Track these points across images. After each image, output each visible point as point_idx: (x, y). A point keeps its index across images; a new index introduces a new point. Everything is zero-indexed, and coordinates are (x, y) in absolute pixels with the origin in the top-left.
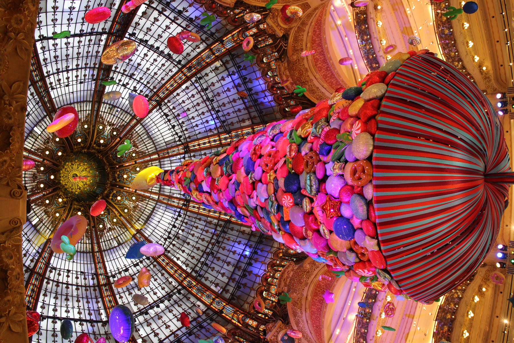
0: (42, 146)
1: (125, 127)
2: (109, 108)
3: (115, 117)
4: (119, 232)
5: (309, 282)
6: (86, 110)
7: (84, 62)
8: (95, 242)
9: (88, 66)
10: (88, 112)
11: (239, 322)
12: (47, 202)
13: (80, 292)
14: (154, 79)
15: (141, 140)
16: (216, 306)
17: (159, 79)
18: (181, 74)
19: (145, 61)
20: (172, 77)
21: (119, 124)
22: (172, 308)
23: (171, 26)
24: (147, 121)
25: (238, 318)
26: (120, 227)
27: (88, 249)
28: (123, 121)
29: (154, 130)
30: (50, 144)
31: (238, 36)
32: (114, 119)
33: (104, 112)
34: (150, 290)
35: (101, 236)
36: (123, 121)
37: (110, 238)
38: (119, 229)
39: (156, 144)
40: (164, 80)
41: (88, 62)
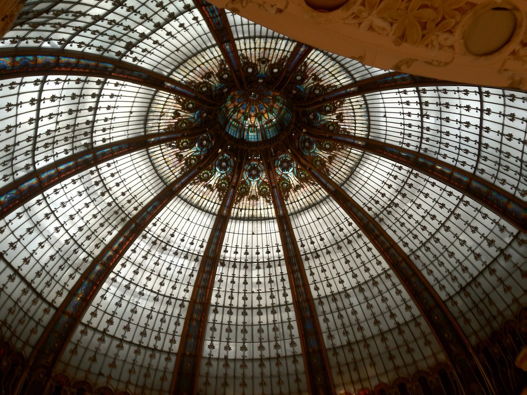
0: (253, 59)
1: (348, 135)
2: (361, 105)
3: (353, 118)
4: (212, 197)
6: (338, 81)
8: (182, 181)
10: (338, 83)
15: (343, 162)
21: (347, 127)
24: (372, 158)
26: (219, 195)
27: (168, 179)
28: (355, 130)
29: (364, 172)
30: (263, 66)
32: (350, 118)
33: (351, 102)
34: (162, 275)
35: (195, 183)
36: (355, 130)
37: (198, 193)
38: (216, 196)
39: (348, 182)
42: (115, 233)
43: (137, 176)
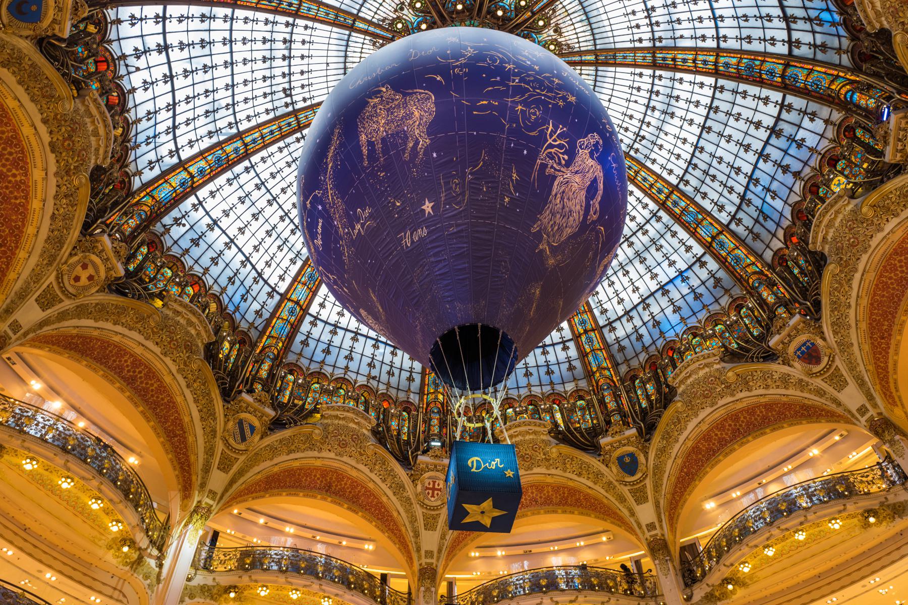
5: (345, 459)
7: (660, 19)
9: (655, 28)
10: (577, 45)
11: (264, 348)
12: (418, 5)
13: (279, 80)
14: (651, 147)
16: (287, 308)
17: (653, 156)
18: (667, 191)
19: (679, 124)
20: (659, 177)
22: (274, 235)
23: (751, 153)
25: (269, 346)
31: (755, 273)
40: (653, 163)
41: (662, 27)
42: (271, 116)
43: (324, 60)
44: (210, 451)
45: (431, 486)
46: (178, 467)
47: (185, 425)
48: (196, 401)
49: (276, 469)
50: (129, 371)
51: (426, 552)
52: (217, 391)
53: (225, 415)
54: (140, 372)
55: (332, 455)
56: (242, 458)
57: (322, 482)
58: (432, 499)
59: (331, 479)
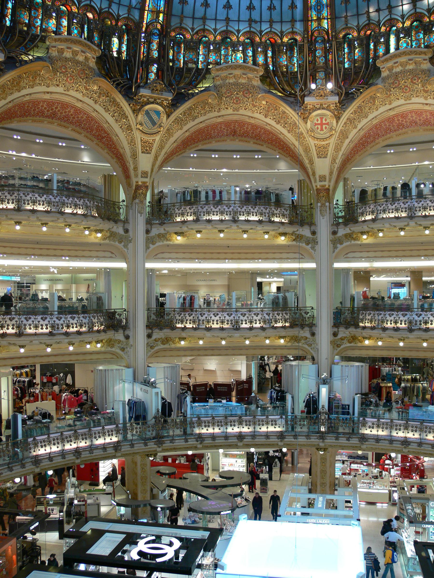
44: (132, 142)
45: (319, 122)
46: (114, 156)
47: (107, 129)
48: (107, 110)
49: (187, 134)
50: (48, 111)
51: (320, 177)
52: (120, 96)
53: (134, 111)
54: (56, 108)
55: (230, 111)
56: (158, 138)
57: (227, 130)
58: (322, 132)
59: (234, 127)
